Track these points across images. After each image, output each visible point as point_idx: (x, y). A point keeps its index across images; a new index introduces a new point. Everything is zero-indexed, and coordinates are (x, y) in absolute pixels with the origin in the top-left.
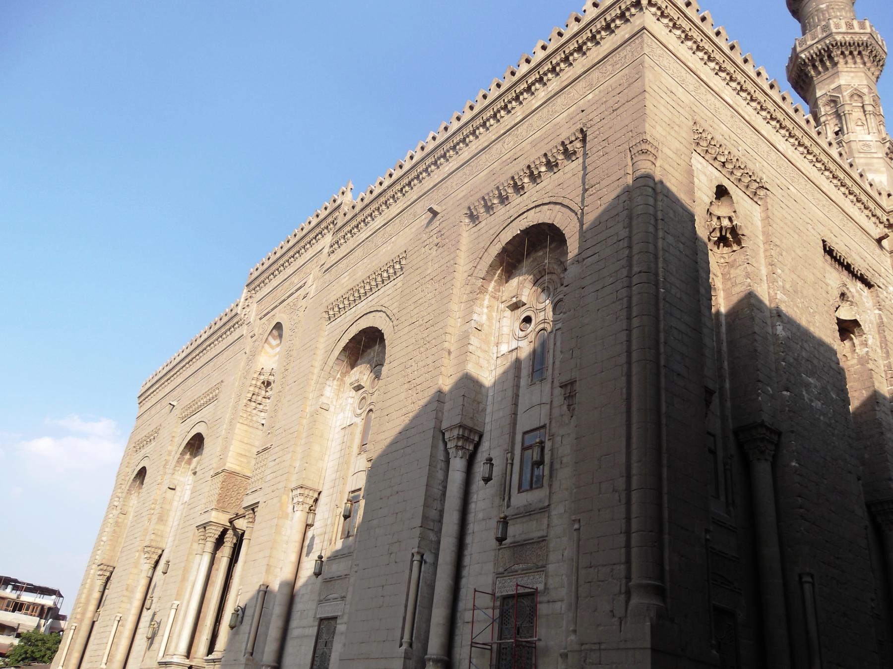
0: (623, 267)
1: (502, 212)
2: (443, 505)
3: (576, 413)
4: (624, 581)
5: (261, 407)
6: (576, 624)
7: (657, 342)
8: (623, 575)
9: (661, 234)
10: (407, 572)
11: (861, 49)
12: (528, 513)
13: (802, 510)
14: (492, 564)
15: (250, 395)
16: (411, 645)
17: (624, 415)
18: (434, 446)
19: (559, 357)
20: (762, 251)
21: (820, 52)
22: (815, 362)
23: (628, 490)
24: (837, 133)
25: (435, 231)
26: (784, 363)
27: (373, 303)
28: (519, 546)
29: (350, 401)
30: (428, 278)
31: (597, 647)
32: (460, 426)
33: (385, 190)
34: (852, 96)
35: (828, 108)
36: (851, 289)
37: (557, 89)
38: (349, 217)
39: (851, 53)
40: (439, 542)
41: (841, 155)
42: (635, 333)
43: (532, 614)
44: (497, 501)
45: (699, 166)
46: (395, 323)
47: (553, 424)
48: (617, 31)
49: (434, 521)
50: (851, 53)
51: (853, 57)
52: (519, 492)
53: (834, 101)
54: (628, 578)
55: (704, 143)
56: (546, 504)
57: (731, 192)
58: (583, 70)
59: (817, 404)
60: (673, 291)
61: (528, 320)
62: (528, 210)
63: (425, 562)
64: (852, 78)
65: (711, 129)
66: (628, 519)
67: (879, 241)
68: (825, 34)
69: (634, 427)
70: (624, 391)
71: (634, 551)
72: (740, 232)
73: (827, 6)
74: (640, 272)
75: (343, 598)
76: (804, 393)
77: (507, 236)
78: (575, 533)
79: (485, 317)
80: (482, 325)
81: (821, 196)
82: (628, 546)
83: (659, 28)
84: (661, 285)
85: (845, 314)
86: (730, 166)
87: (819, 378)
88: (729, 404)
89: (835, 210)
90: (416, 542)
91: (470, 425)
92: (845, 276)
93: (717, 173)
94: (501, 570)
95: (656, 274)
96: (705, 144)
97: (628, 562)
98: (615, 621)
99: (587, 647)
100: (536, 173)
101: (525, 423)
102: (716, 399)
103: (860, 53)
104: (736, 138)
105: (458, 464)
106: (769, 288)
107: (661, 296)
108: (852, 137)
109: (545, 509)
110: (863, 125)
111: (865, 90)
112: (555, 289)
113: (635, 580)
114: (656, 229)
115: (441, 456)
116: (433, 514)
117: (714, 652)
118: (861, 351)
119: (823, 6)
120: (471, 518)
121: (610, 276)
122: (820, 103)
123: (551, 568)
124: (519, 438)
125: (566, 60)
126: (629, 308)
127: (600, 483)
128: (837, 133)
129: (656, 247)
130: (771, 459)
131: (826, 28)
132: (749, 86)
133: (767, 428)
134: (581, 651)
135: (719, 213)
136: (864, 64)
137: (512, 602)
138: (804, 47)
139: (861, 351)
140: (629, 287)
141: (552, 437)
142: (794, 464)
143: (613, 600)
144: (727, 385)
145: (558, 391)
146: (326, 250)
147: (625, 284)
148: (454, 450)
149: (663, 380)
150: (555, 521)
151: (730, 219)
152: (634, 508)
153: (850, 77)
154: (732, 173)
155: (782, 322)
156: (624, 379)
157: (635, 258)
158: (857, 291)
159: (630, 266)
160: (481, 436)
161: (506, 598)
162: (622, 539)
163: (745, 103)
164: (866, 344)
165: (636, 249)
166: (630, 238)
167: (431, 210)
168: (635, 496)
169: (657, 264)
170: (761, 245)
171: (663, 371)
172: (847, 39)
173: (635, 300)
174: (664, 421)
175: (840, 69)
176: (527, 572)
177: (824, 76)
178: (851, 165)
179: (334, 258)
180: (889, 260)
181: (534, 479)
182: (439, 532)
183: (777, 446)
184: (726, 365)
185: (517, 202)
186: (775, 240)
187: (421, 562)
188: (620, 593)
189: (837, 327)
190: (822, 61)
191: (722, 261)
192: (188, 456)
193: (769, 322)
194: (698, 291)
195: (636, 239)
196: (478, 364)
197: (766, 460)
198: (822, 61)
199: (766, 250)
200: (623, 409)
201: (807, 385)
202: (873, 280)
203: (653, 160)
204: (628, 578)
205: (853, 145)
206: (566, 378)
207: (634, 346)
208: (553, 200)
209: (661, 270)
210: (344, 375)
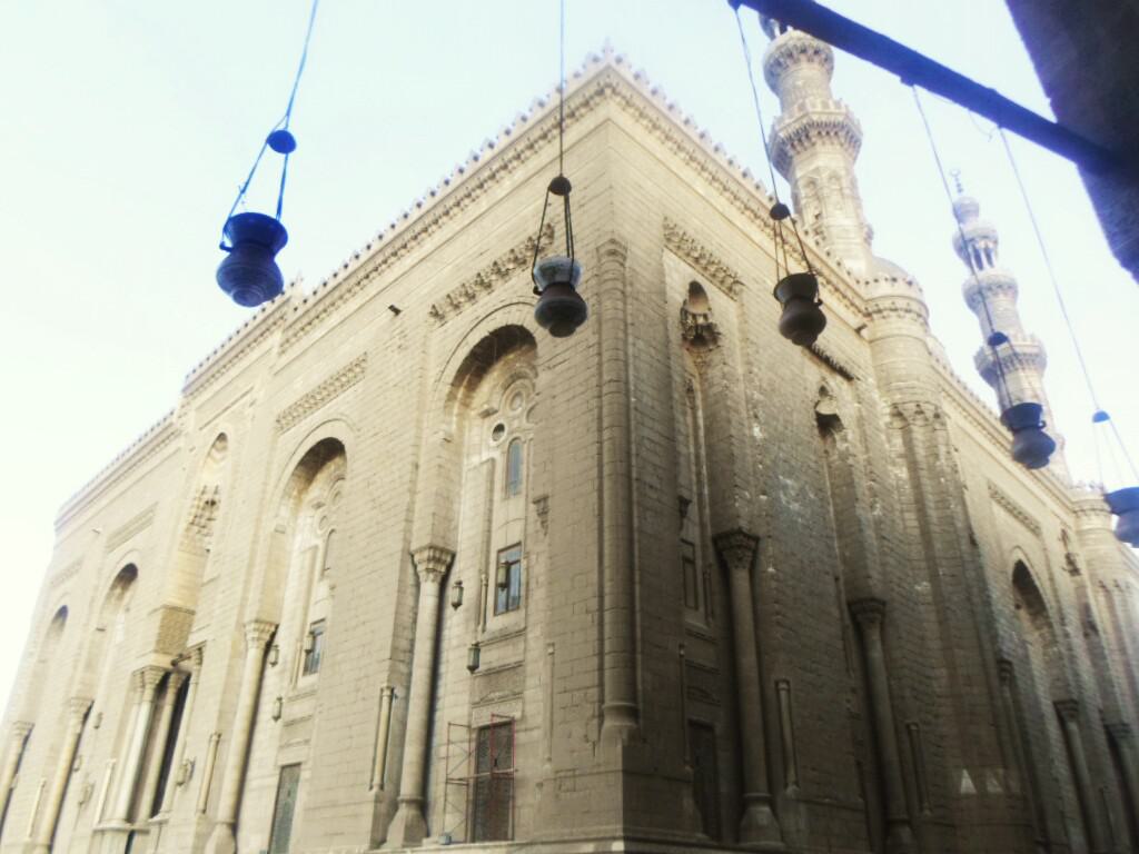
0: (594, 376)
1: (470, 312)
2: (414, 632)
3: (549, 530)
4: (597, 705)
5: (205, 531)
6: (551, 753)
7: (629, 454)
8: (596, 698)
9: (631, 339)
10: (376, 709)
12: (505, 637)
13: (779, 617)
14: (468, 693)
15: (191, 518)
16: (382, 787)
17: (596, 532)
18: (403, 570)
19: (533, 470)
20: (738, 351)
22: (793, 462)
23: (601, 609)
24: (817, 217)
25: (398, 331)
26: (760, 466)
27: (332, 410)
28: (493, 673)
29: (309, 520)
30: (391, 384)
31: (570, 773)
32: (431, 547)
33: (340, 284)
34: (830, 178)
35: (808, 190)
37: (522, 178)
38: (300, 312)
39: (828, 133)
40: (410, 674)
41: (817, 243)
42: (606, 445)
43: (510, 744)
44: (472, 625)
46: (357, 433)
47: (529, 541)
48: (583, 120)
49: (405, 652)
50: (828, 133)
52: (495, 614)
53: (812, 183)
54: (602, 701)
55: (674, 238)
56: (522, 626)
58: (548, 160)
59: (795, 506)
60: (645, 399)
61: (500, 428)
62: (496, 310)
63: (396, 697)
66: (601, 640)
67: (858, 331)
68: (802, 114)
69: (607, 544)
70: (596, 507)
71: (607, 674)
73: (805, 83)
74: (610, 381)
75: (307, 742)
76: (782, 496)
77: (475, 339)
78: (549, 657)
79: (454, 427)
80: (451, 436)
82: (601, 669)
83: (625, 119)
84: (632, 393)
85: (825, 409)
86: (703, 262)
87: (797, 479)
88: (707, 511)
90: (385, 676)
91: (441, 545)
92: (825, 371)
93: (690, 270)
94: (477, 699)
95: (627, 383)
96: (676, 239)
97: (601, 685)
98: (589, 746)
99: (562, 774)
100: (503, 270)
101: (498, 541)
102: (693, 510)
103: (836, 133)
105: (429, 588)
106: (746, 388)
107: (632, 406)
109: (521, 633)
110: (841, 209)
111: (843, 173)
112: (528, 395)
113: (608, 703)
114: (626, 334)
115: (411, 580)
116: (404, 644)
117: (688, 768)
118: (841, 446)
119: (800, 83)
120: (445, 645)
121: (581, 384)
122: (801, 183)
123: (528, 694)
124: (493, 556)
125: (531, 147)
126: (600, 419)
127: (574, 604)
128: (817, 217)
129: (626, 354)
130: (748, 566)
131: (802, 107)
132: (721, 176)
133: (745, 535)
134: (555, 779)
136: (842, 145)
137: (488, 733)
138: (782, 125)
139: (841, 446)
140: (600, 397)
141: (527, 556)
142: (771, 570)
143: (587, 724)
144: (706, 491)
145: (532, 507)
146: (276, 350)
147: (596, 394)
148: (424, 573)
149: (635, 495)
150: (532, 644)
151: (705, 316)
152: (607, 628)
154: (705, 269)
155: (759, 423)
156: (595, 494)
157: (605, 366)
158: (837, 385)
159: (600, 375)
160: (453, 556)
161: (482, 729)
162: (595, 660)
163: (715, 193)
165: (606, 356)
166: (600, 344)
167: (392, 308)
168: (608, 617)
169: (627, 370)
170: (738, 343)
171: (635, 485)
173: (605, 411)
174: (636, 536)
176: (503, 699)
177: (804, 155)
178: (828, 254)
179: (285, 359)
180: (868, 350)
181: (510, 601)
182: (410, 663)
183: (755, 552)
184: (704, 471)
185: (486, 301)
186: (752, 338)
187: (392, 696)
188: (593, 716)
189: (815, 423)
190: (800, 140)
191: (699, 360)
192: (118, 591)
193: (746, 423)
194: (671, 398)
195: (605, 345)
196: (448, 478)
197: (744, 567)
198: (800, 140)
199: (742, 348)
200: (596, 525)
201: (785, 487)
202: (854, 371)
203: (621, 260)
204: (602, 701)
205: (832, 229)
206: (539, 492)
207: (606, 459)
208: (521, 300)
209: (631, 378)
210: (300, 492)
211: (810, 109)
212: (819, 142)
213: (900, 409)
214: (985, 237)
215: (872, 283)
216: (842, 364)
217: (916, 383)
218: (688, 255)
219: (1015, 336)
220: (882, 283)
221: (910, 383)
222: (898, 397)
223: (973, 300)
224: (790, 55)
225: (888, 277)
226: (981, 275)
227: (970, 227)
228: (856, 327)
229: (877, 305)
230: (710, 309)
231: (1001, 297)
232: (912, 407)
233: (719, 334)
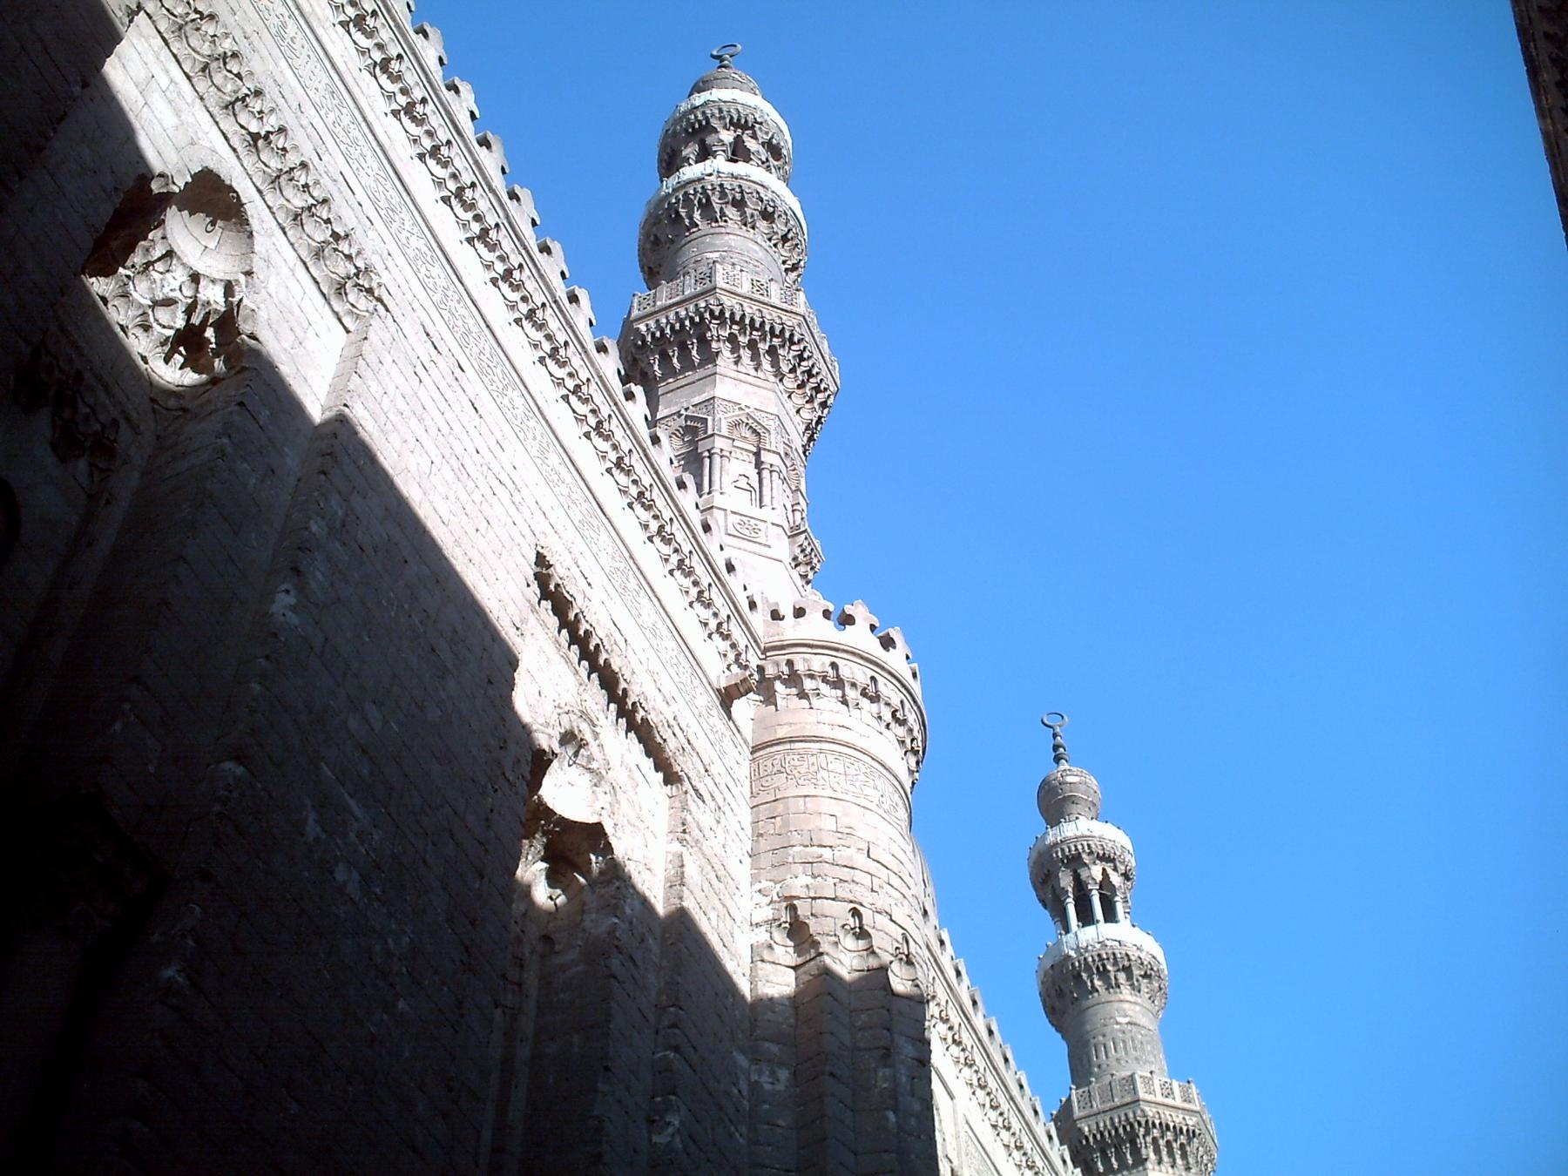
11: (776, 341)
21: (682, 325)
26: (257, 687)
36: (603, 738)
39: (752, 345)
45: (164, 81)
51: (755, 357)
57: (255, 224)
64: (747, 394)
65: (238, 35)
72: (245, 327)
81: (567, 475)
89: (605, 540)
104: (320, 126)
108: (718, 500)
111: (772, 425)
135: (200, 267)
142: (169, 972)
151: (229, 289)
153: (739, 388)
155: (301, 589)
164: (616, 907)
172: (748, 310)
175: (718, 370)
180: (744, 770)
202: (682, 764)
211: (720, 280)
212: (726, 349)
213: (803, 909)
214: (1104, 858)
215: (786, 610)
216: (653, 718)
217: (861, 860)
218: (229, 106)
219: (1148, 1082)
220: (814, 618)
221: (843, 855)
222: (798, 883)
223: (1060, 993)
224: (706, 207)
225: (831, 608)
226: (1087, 935)
227: (1080, 828)
228: (723, 684)
229: (790, 663)
230: (249, 273)
231: (1126, 992)
232: (841, 910)
233: (253, 337)
